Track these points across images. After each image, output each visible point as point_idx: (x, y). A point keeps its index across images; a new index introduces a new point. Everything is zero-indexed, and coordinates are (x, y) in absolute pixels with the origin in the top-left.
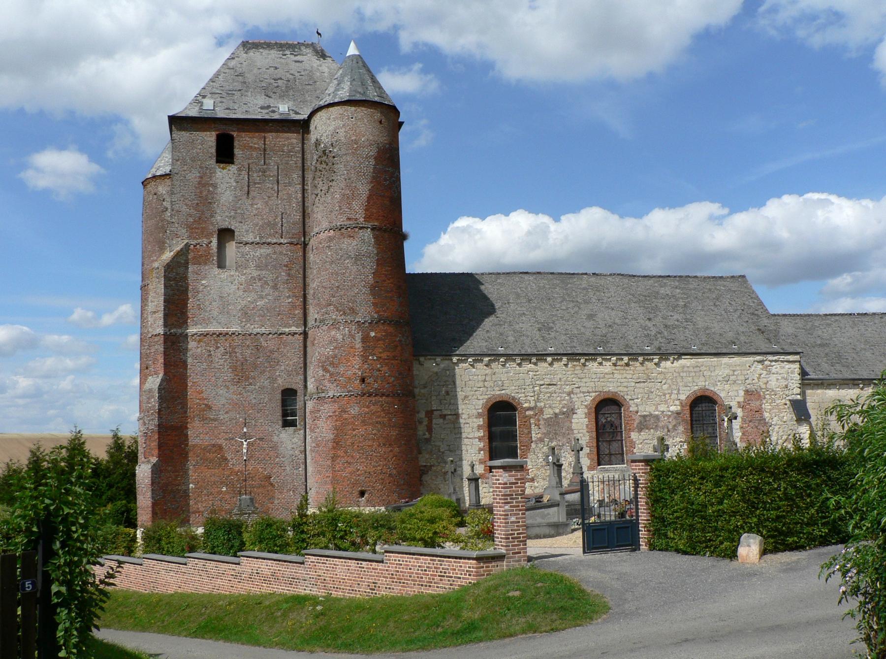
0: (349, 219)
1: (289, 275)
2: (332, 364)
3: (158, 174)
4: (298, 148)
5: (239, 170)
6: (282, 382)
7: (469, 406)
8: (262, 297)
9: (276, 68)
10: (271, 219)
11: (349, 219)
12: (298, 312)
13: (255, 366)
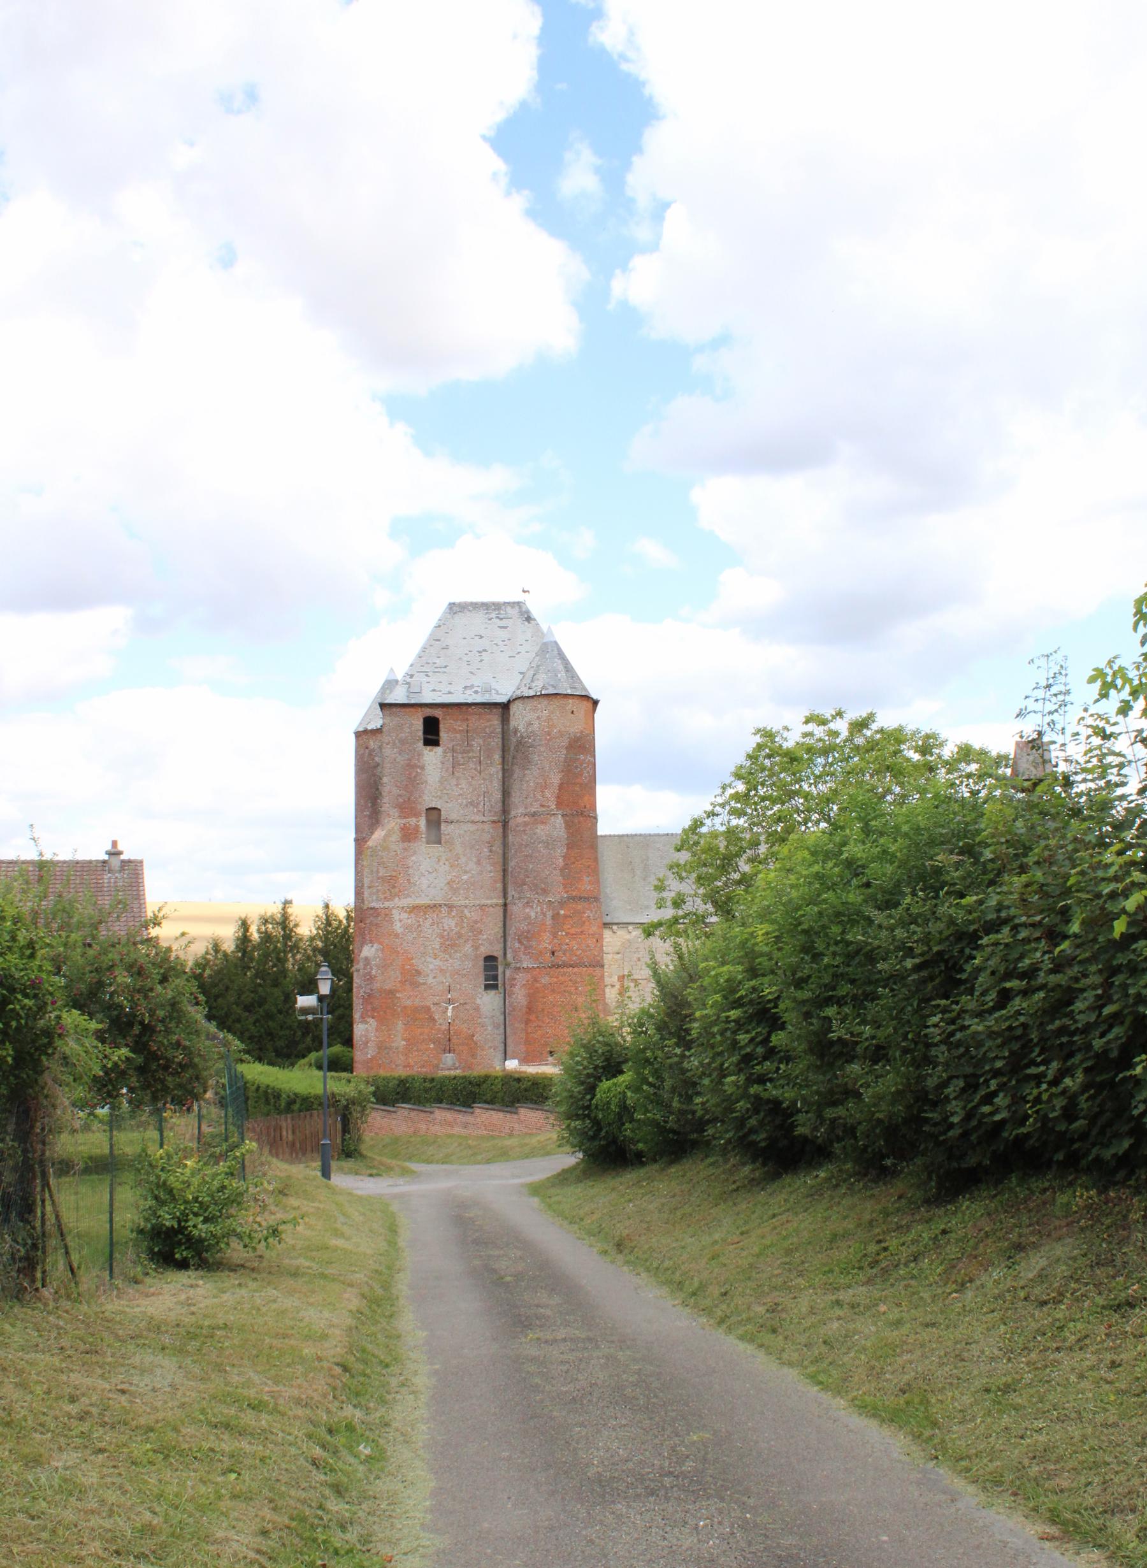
0: (542, 806)
1: (491, 851)
2: (526, 937)
3: (369, 728)
4: (499, 730)
5: (445, 752)
6: (485, 950)
8: (466, 872)
9: (481, 637)
10: (474, 798)
11: (542, 806)
12: (499, 885)
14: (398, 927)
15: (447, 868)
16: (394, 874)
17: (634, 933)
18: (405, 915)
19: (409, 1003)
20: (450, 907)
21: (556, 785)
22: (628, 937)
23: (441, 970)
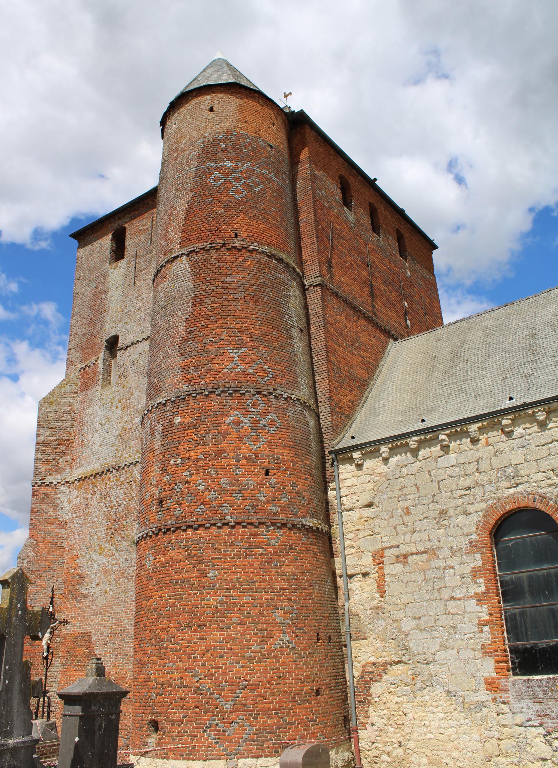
7: (451, 530)
14: (66, 513)
15: (119, 412)
16: (66, 436)
17: (393, 460)
18: (74, 493)
20: (118, 468)
21: (182, 215)
22: (383, 468)
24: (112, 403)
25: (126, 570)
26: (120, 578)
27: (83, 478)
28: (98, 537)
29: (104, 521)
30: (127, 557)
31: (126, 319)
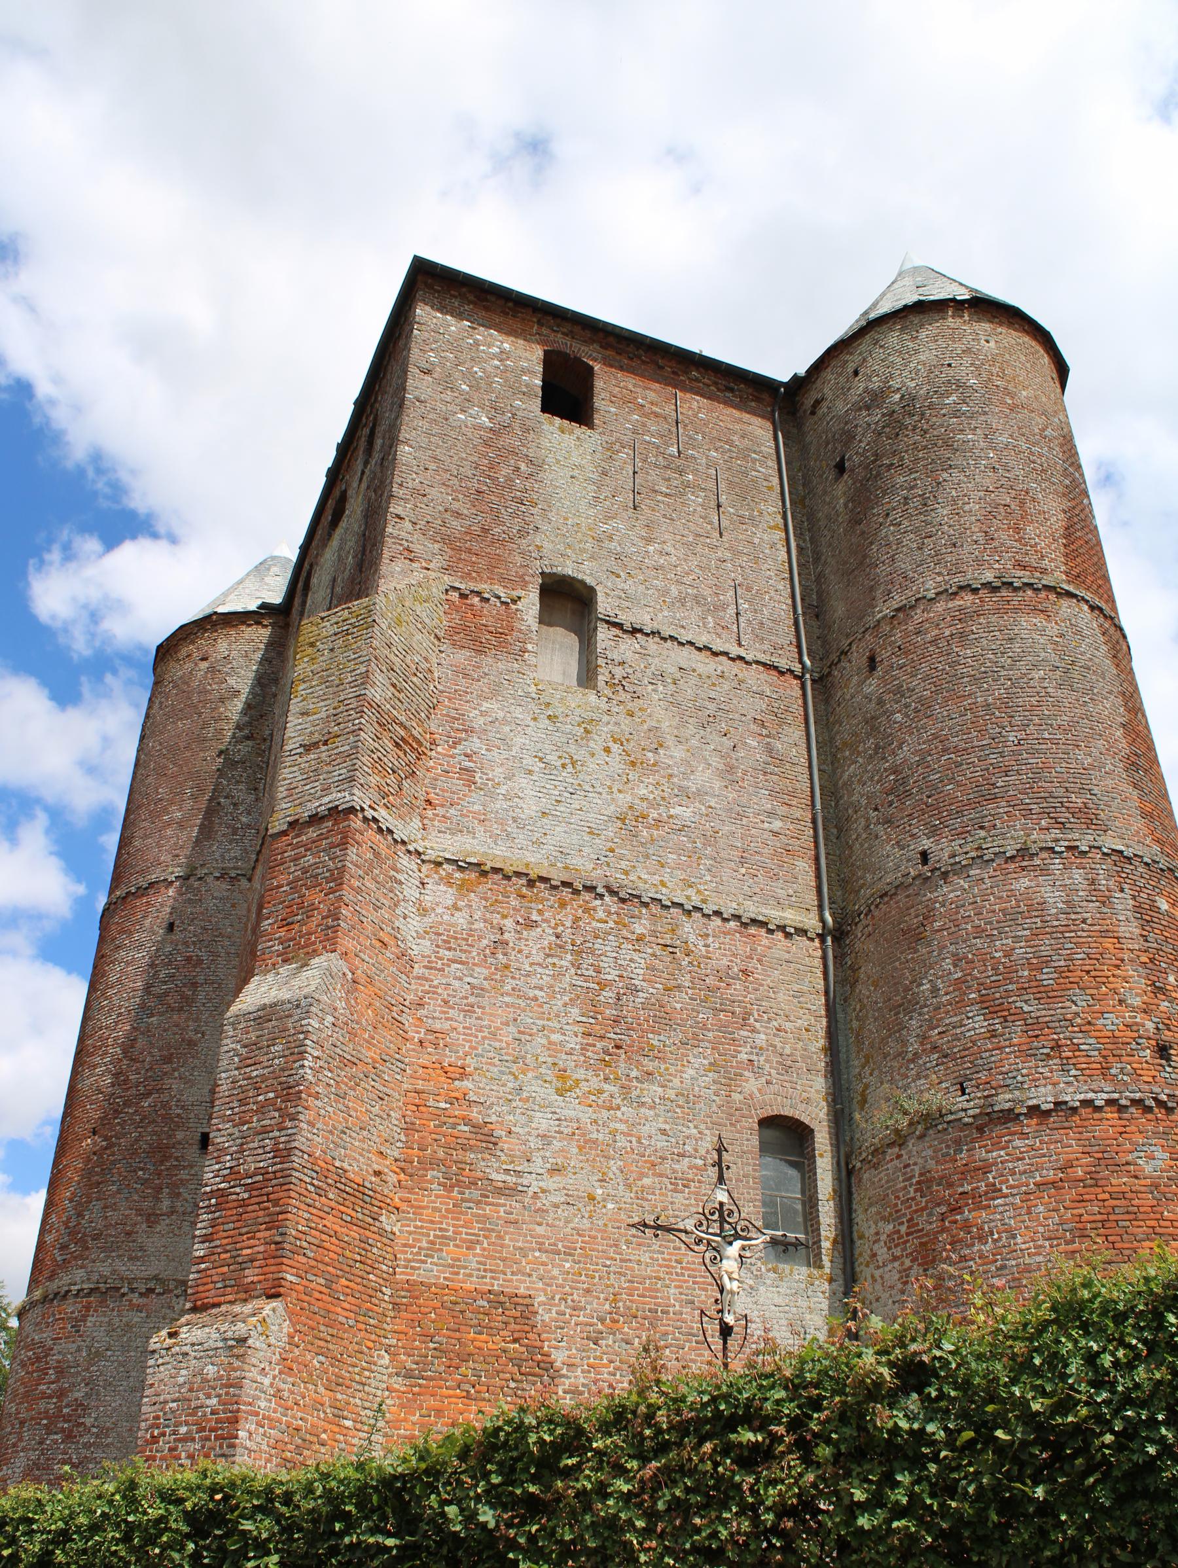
1: (770, 750)
8: (686, 795)
13: (664, 1019)
15: (616, 763)
18: (448, 895)
19: (431, 1271)
23: (588, 1144)
24: (587, 731)
25: (663, 1158)
26: (642, 1176)
27: (487, 868)
28: (550, 1043)
29: (575, 1011)
30: (667, 1127)
31: (612, 564)
